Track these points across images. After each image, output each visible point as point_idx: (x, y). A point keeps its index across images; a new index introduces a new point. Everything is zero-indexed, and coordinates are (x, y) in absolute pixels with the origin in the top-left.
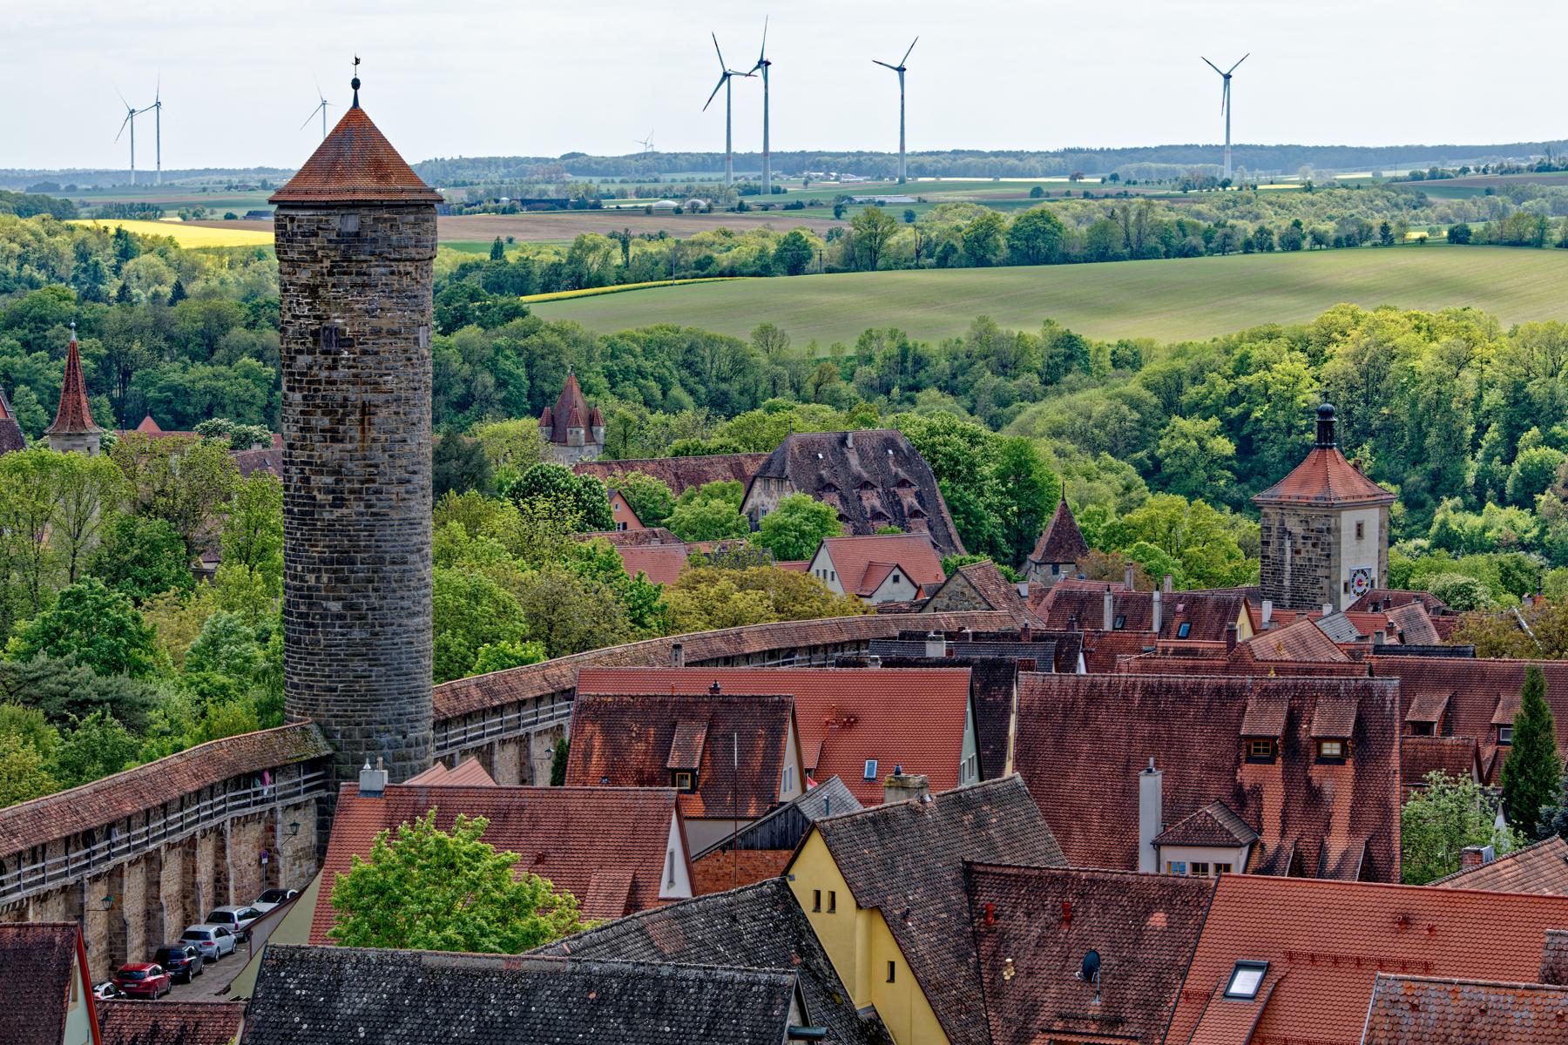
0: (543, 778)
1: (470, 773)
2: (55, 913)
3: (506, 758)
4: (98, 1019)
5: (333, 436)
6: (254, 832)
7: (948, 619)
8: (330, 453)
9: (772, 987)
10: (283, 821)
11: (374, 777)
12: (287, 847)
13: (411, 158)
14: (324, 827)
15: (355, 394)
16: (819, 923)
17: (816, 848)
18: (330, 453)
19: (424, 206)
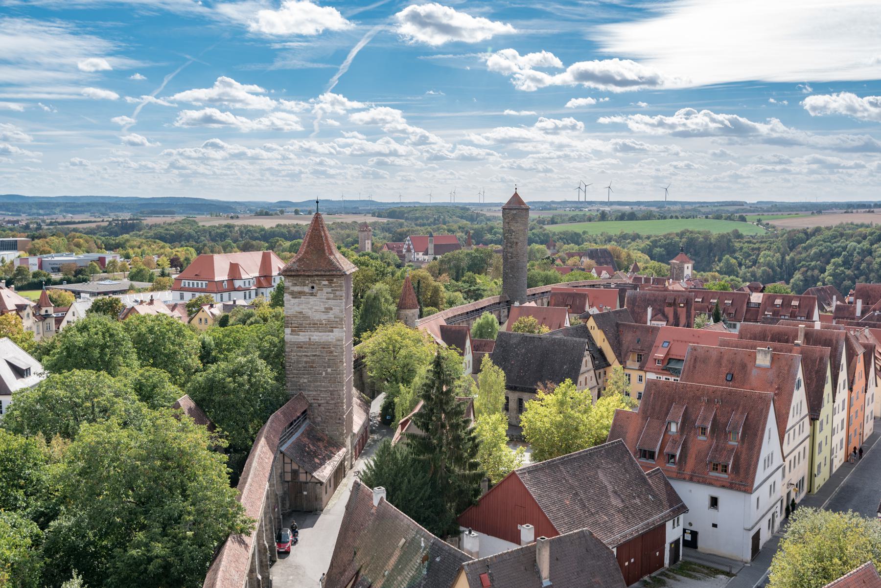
0: (545, 306)
1: (533, 304)
2: (465, 325)
3: (539, 301)
4: (472, 342)
5: (511, 247)
6: (497, 312)
7: (616, 281)
8: (511, 250)
9: (584, 342)
10: (502, 311)
11: (517, 304)
12: (502, 315)
13: (525, 201)
14: (509, 312)
15: (515, 240)
16: (592, 331)
17: (591, 319)
18: (511, 250)
19: (527, 209)
